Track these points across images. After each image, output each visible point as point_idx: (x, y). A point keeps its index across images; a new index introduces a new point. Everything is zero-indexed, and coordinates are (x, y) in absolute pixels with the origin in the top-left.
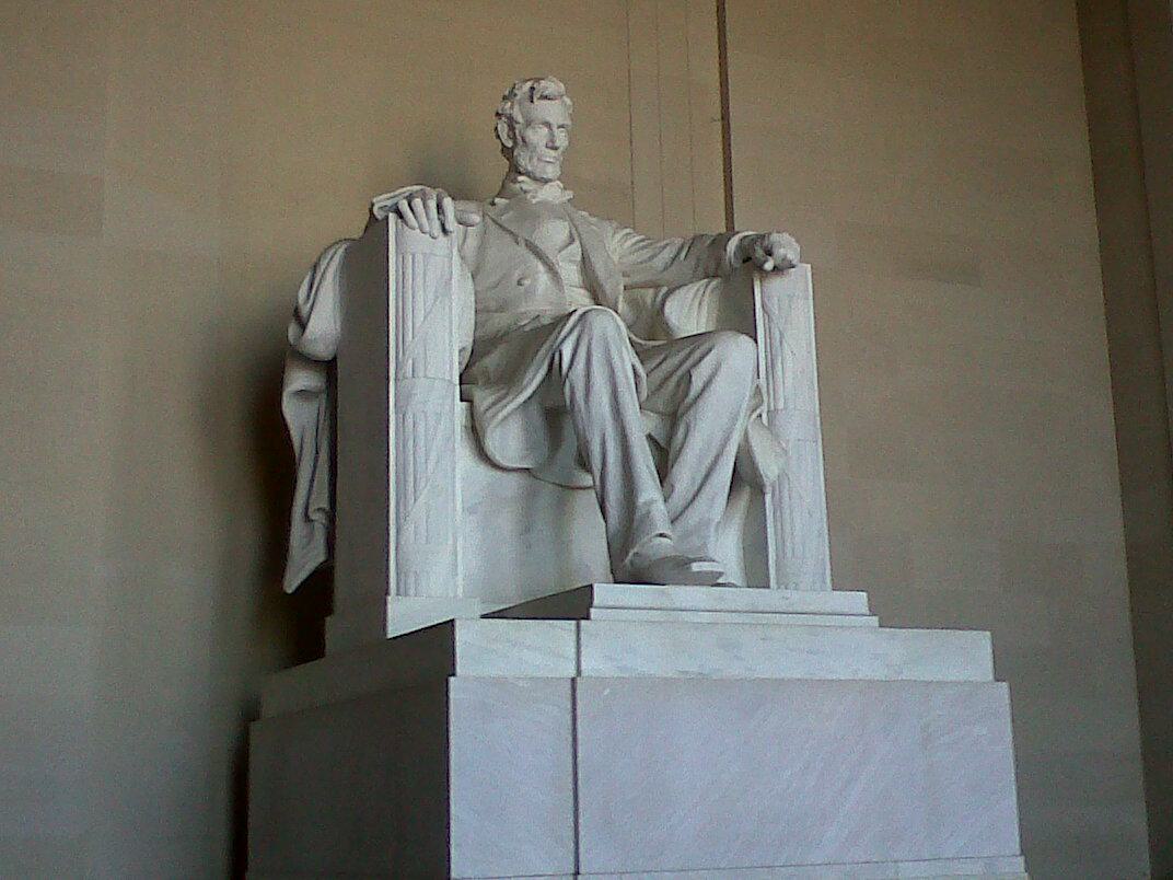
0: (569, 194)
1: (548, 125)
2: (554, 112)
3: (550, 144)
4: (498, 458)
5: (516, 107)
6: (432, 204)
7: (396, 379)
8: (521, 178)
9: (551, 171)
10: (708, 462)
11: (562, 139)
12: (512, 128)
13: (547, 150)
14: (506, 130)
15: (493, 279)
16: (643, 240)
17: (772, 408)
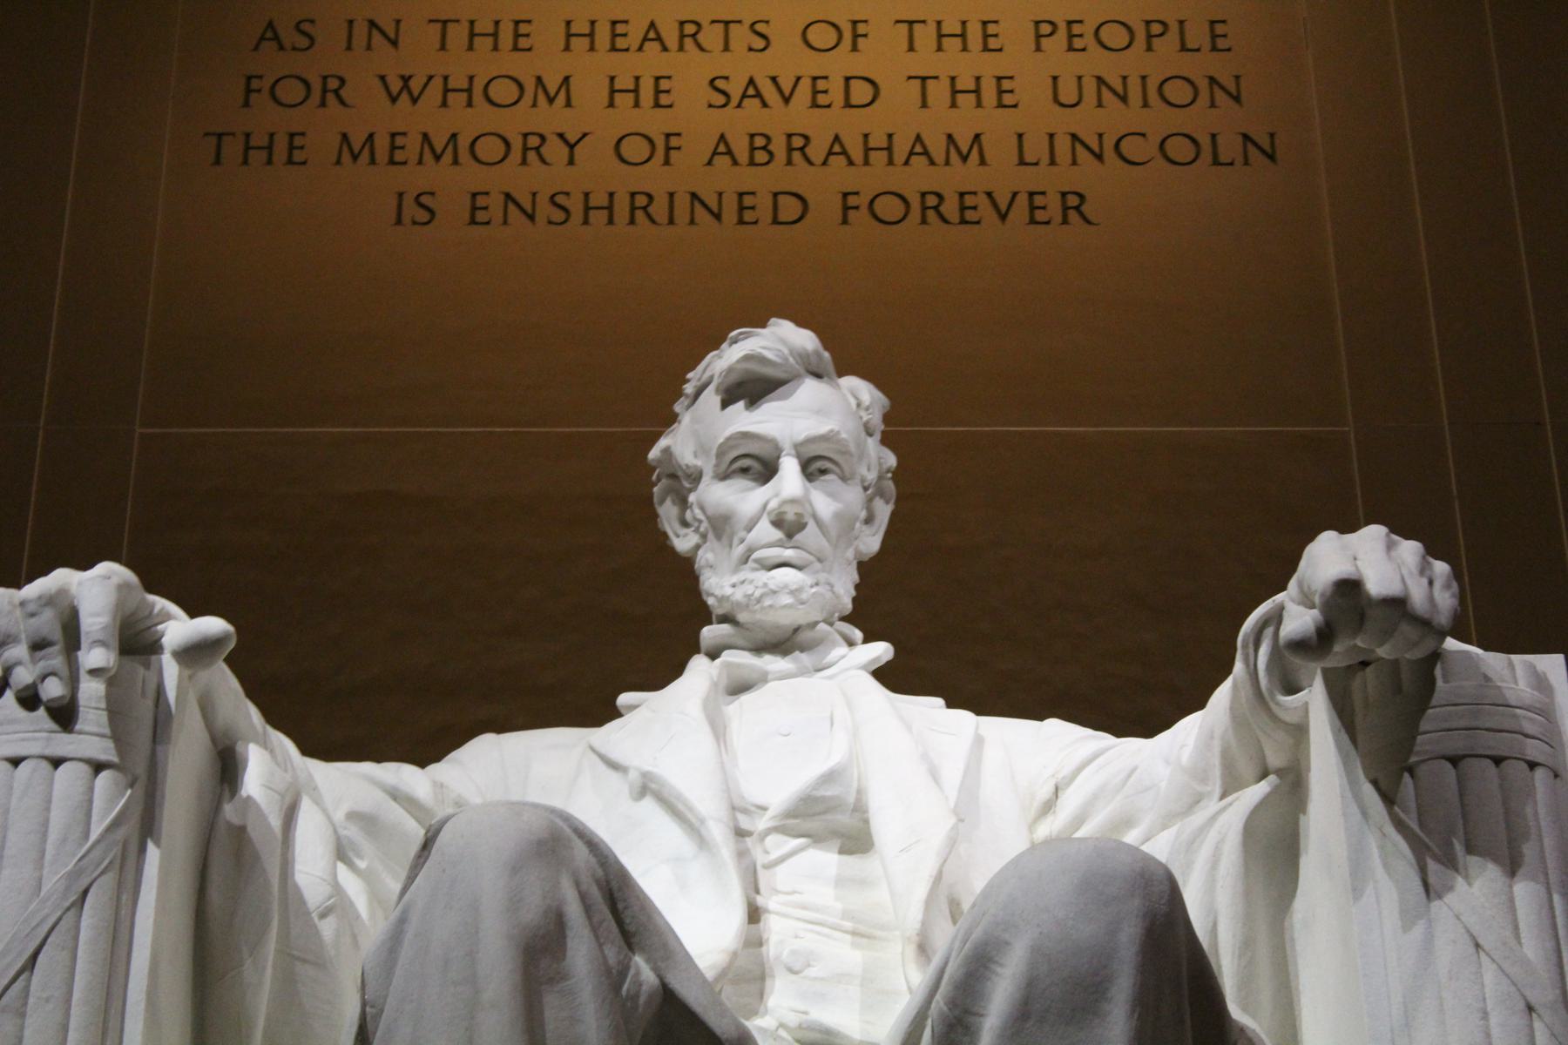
0: (881, 651)
3: (773, 504)
8: (709, 633)
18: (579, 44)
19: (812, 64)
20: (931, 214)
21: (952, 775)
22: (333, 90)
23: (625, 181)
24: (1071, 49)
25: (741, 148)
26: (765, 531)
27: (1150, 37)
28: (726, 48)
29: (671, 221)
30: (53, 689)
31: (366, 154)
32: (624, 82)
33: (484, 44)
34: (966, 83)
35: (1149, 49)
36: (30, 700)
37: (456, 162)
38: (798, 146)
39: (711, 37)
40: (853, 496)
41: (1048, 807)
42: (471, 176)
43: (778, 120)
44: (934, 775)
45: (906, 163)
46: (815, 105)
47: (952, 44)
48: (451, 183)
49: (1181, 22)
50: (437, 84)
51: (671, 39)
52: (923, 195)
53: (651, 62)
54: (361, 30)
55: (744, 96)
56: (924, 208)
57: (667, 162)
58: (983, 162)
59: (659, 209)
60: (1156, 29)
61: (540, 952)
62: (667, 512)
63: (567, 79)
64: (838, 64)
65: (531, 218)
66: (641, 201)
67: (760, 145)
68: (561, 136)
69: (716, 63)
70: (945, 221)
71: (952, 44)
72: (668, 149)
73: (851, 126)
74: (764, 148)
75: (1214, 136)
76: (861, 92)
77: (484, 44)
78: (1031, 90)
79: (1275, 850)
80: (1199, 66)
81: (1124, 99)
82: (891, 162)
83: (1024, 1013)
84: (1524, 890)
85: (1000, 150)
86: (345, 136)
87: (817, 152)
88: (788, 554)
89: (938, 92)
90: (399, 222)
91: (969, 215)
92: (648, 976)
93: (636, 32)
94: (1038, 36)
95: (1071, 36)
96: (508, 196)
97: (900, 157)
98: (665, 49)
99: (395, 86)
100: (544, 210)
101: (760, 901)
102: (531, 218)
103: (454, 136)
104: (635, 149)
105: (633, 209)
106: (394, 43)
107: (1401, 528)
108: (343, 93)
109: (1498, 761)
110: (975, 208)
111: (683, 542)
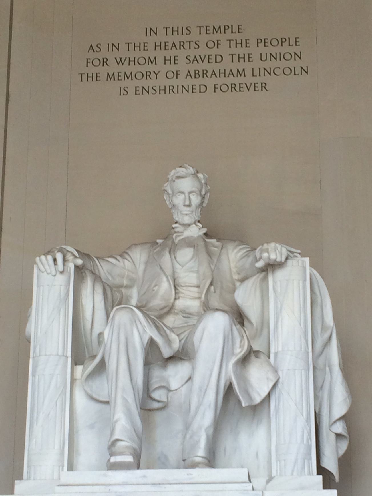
0: (204, 230)
1: (182, 193)
2: (187, 185)
4: (94, 396)
5: (169, 186)
6: (50, 258)
7: (33, 357)
8: (174, 226)
9: (187, 220)
10: (203, 390)
11: (195, 200)
12: (169, 197)
13: (186, 208)
14: (168, 199)
15: (146, 287)
16: (247, 251)
17: (276, 351)
18: (158, 48)
19: (208, 52)
20: (233, 89)
22: (105, 62)
23: (168, 83)
24: (265, 46)
25: (193, 75)
27: (282, 42)
28: (190, 48)
29: (178, 92)
30: (54, 274)
31: (113, 78)
32: (168, 58)
33: (137, 49)
34: (242, 56)
35: (282, 45)
37: (132, 79)
38: (205, 73)
39: (187, 45)
40: (200, 198)
42: (135, 83)
43: (200, 66)
45: (228, 76)
46: (209, 62)
47: (239, 46)
48: (131, 84)
49: (289, 39)
50: (128, 59)
51: (178, 47)
52: (232, 84)
53: (174, 52)
54: (111, 45)
55: (194, 60)
56: (232, 87)
57: (177, 78)
58: (245, 76)
59: (175, 90)
60: (284, 40)
63: (155, 58)
64: (214, 52)
65: (148, 93)
66: (171, 88)
67: (197, 72)
68: (154, 72)
69: (188, 52)
70: (235, 90)
71: (239, 46)
72: (177, 74)
73: (216, 67)
74: (198, 74)
75: (295, 68)
76: (219, 59)
77: (137, 49)
78: (256, 57)
80: (292, 50)
81: (276, 59)
82: (225, 76)
85: (248, 72)
86: (108, 74)
87: (209, 74)
88: (188, 213)
89: (236, 58)
90: (120, 94)
91: (241, 89)
93: (170, 45)
94: (258, 42)
95: (265, 42)
96: (143, 87)
97: (227, 75)
98: (176, 49)
99: (119, 60)
100: (151, 90)
101: (178, 288)
102: (148, 93)
103: (131, 73)
104: (170, 75)
105: (170, 89)
106: (118, 49)
108: (107, 63)
110: (242, 87)
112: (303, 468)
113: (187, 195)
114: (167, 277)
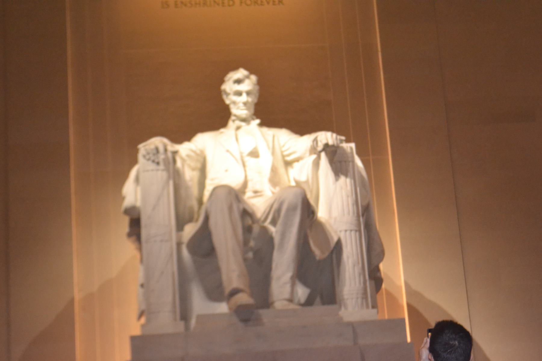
0: (258, 121)
8: (233, 118)
21: (271, 145)
26: (241, 105)
30: (156, 161)
36: (153, 161)
41: (283, 146)
44: (269, 148)
61: (230, 208)
62: (224, 97)
79: (316, 164)
83: (288, 210)
84: (348, 180)
92: (241, 207)
107: (333, 131)
109: (345, 162)
111: (227, 102)
112: (362, 304)
113: (244, 95)
114: (236, 160)
